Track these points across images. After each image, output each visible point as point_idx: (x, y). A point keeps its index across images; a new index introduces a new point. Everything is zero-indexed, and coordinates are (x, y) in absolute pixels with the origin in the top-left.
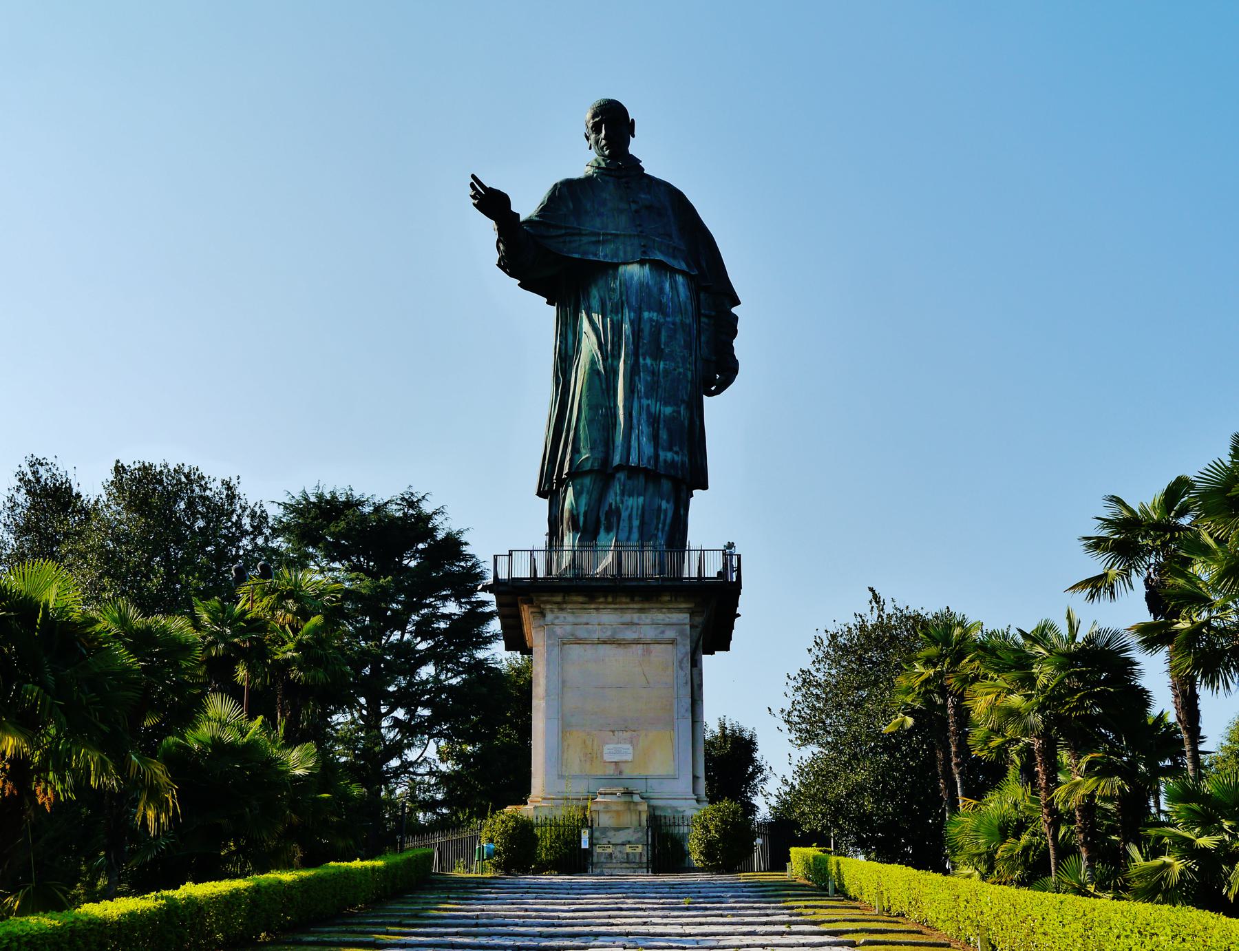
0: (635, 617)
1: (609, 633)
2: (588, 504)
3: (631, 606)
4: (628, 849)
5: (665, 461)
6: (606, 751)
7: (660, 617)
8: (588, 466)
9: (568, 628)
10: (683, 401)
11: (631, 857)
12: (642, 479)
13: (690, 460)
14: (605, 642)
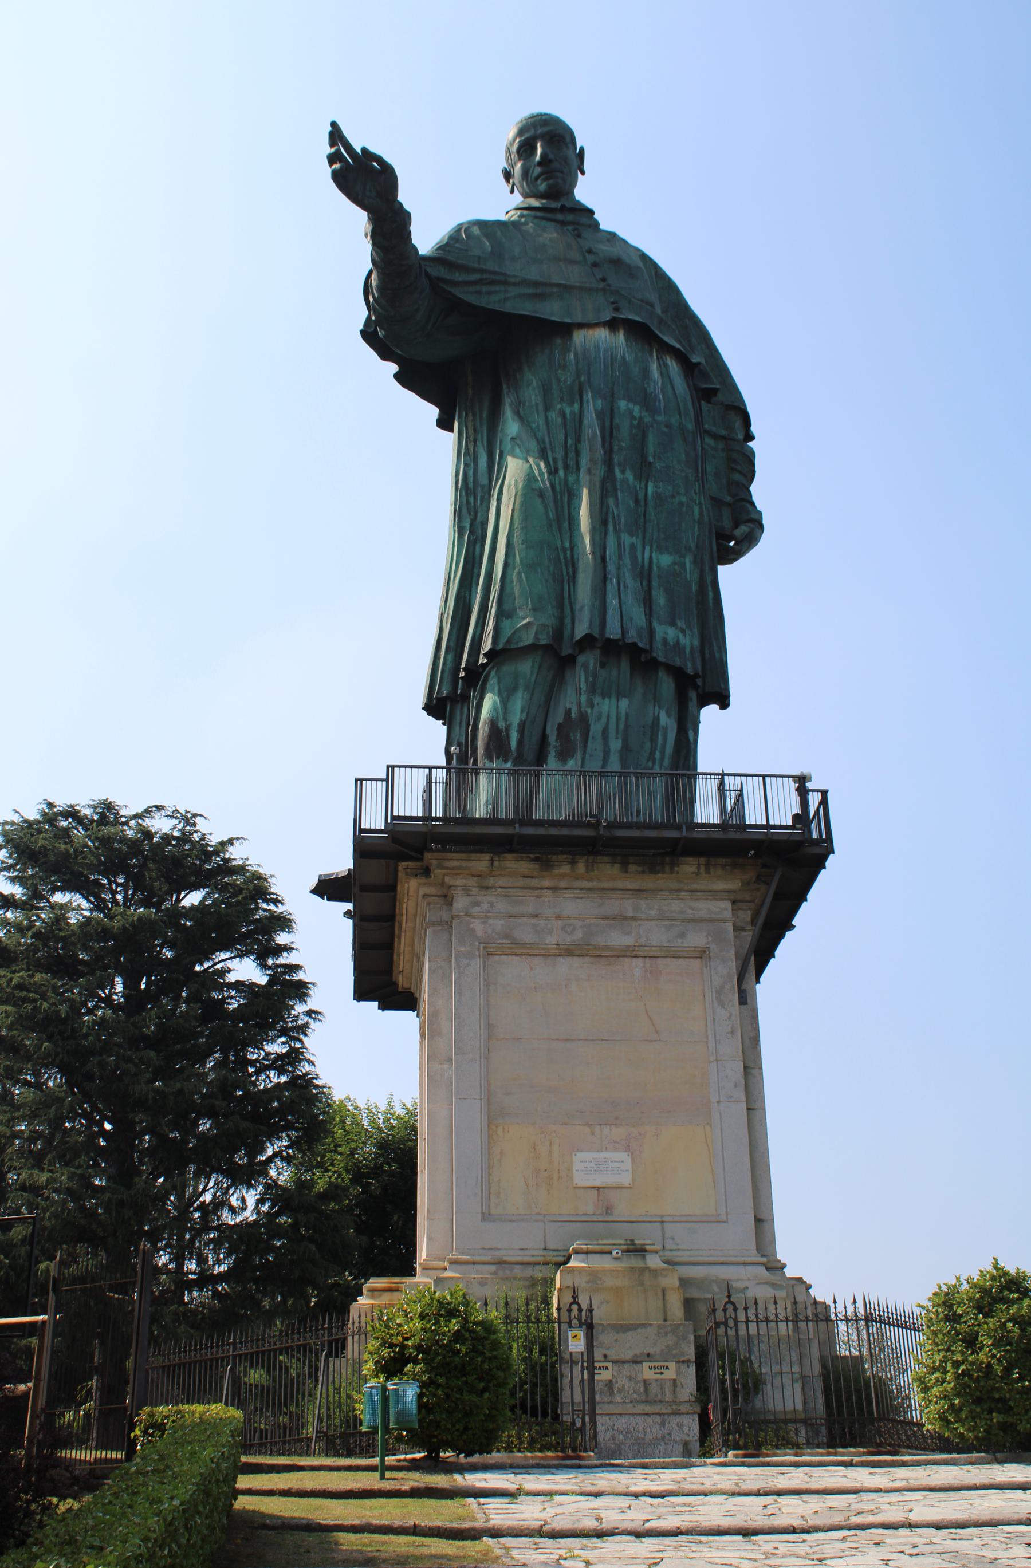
0: (628, 906)
1: (578, 935)
3: (620, 884)
4: (646, 1372)
6: (577, 1166)
7: (675, 906)
8: (528, 639)
9: (499, 924)
10: (688, 549)
11: (654, 1389)
12: (625, 665)
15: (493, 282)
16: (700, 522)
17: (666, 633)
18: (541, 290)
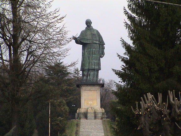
18: (88, 40)
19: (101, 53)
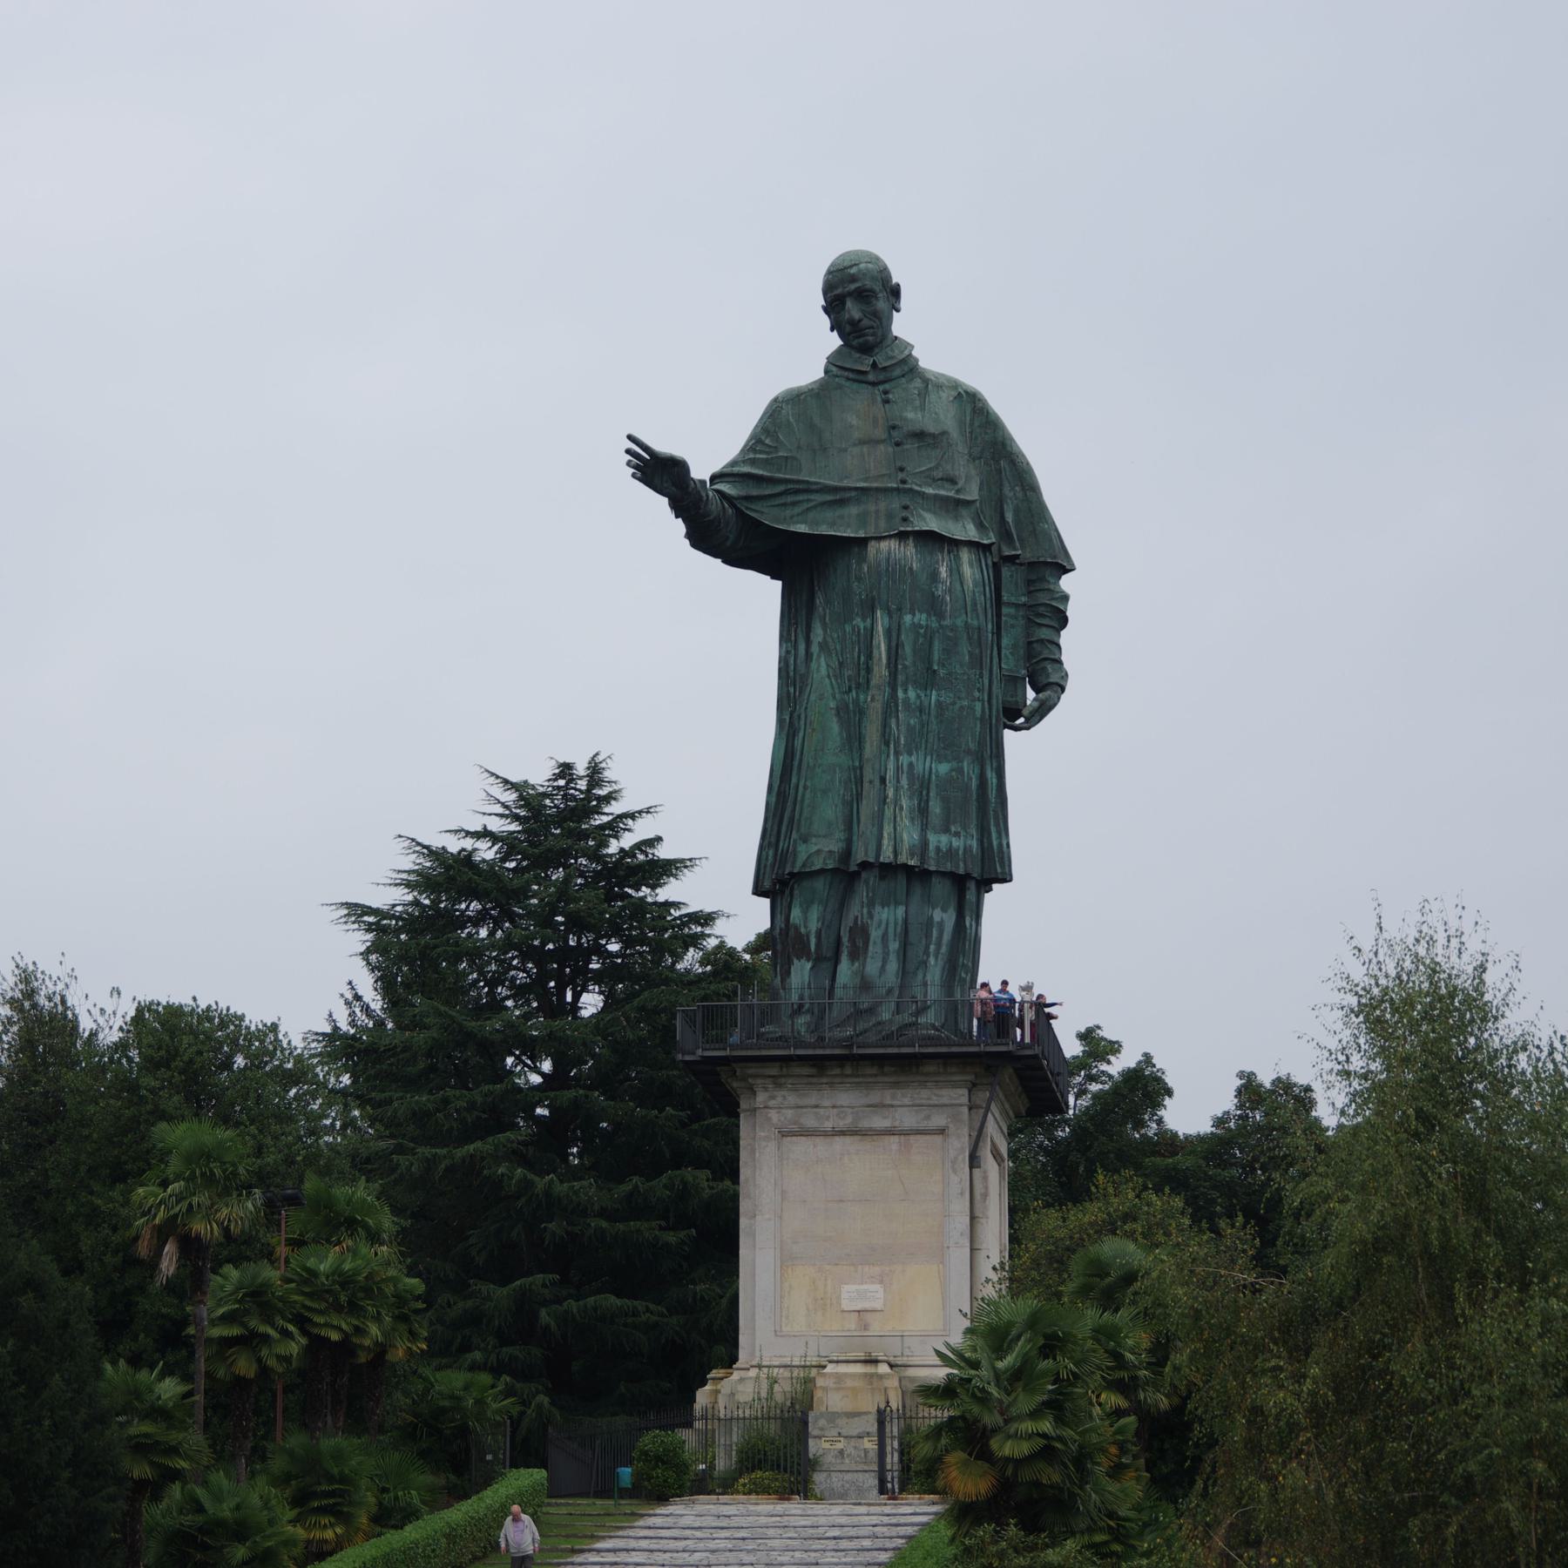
0: (887, 1096)
1: (849, 1120)
2: (822, 919)
3: (880, 1079)
5: (938, 849)
7: (924, 1095)
9: (789, 1113)
10: (968, 752)
13: (981, 842)
14: (842, 1133)
15: (797, 492)
16: (982, 719)
17: (937, 840)
18: (840, 497)
19: (1011, 662)
